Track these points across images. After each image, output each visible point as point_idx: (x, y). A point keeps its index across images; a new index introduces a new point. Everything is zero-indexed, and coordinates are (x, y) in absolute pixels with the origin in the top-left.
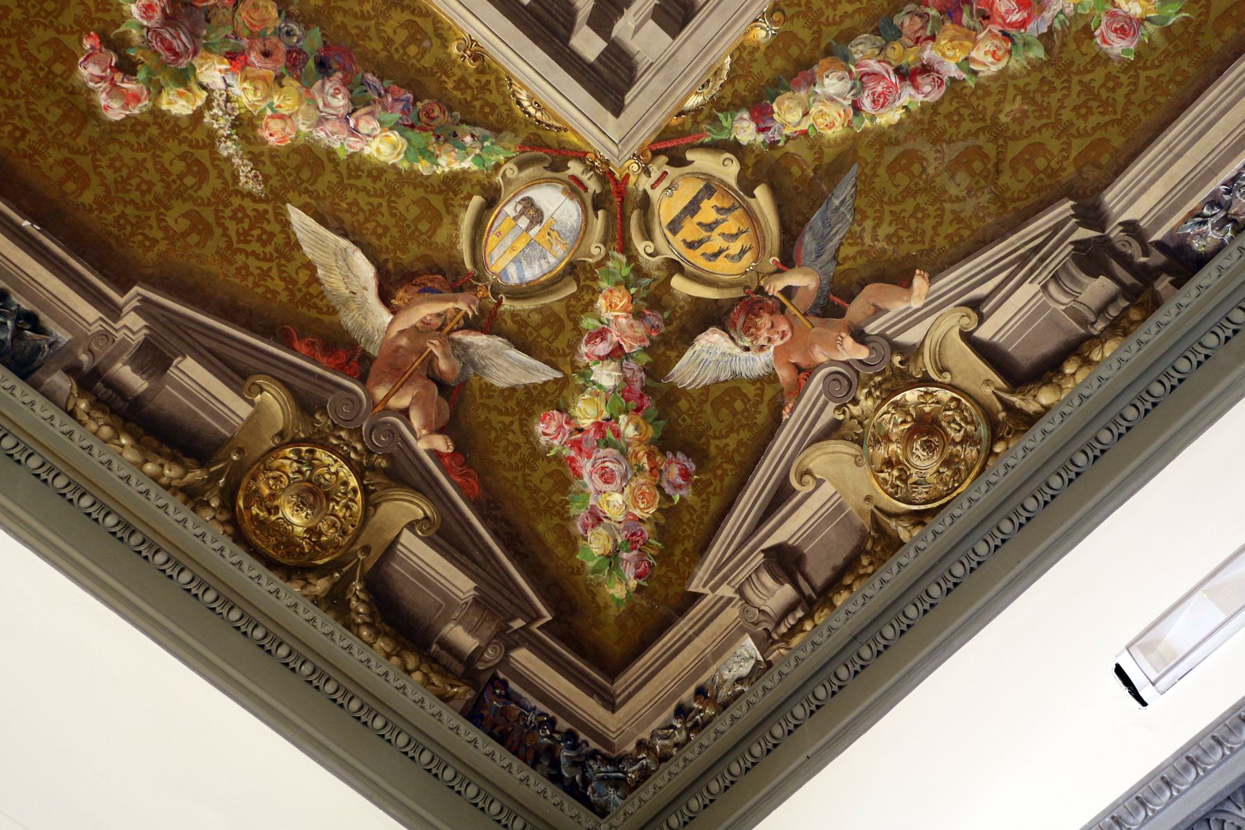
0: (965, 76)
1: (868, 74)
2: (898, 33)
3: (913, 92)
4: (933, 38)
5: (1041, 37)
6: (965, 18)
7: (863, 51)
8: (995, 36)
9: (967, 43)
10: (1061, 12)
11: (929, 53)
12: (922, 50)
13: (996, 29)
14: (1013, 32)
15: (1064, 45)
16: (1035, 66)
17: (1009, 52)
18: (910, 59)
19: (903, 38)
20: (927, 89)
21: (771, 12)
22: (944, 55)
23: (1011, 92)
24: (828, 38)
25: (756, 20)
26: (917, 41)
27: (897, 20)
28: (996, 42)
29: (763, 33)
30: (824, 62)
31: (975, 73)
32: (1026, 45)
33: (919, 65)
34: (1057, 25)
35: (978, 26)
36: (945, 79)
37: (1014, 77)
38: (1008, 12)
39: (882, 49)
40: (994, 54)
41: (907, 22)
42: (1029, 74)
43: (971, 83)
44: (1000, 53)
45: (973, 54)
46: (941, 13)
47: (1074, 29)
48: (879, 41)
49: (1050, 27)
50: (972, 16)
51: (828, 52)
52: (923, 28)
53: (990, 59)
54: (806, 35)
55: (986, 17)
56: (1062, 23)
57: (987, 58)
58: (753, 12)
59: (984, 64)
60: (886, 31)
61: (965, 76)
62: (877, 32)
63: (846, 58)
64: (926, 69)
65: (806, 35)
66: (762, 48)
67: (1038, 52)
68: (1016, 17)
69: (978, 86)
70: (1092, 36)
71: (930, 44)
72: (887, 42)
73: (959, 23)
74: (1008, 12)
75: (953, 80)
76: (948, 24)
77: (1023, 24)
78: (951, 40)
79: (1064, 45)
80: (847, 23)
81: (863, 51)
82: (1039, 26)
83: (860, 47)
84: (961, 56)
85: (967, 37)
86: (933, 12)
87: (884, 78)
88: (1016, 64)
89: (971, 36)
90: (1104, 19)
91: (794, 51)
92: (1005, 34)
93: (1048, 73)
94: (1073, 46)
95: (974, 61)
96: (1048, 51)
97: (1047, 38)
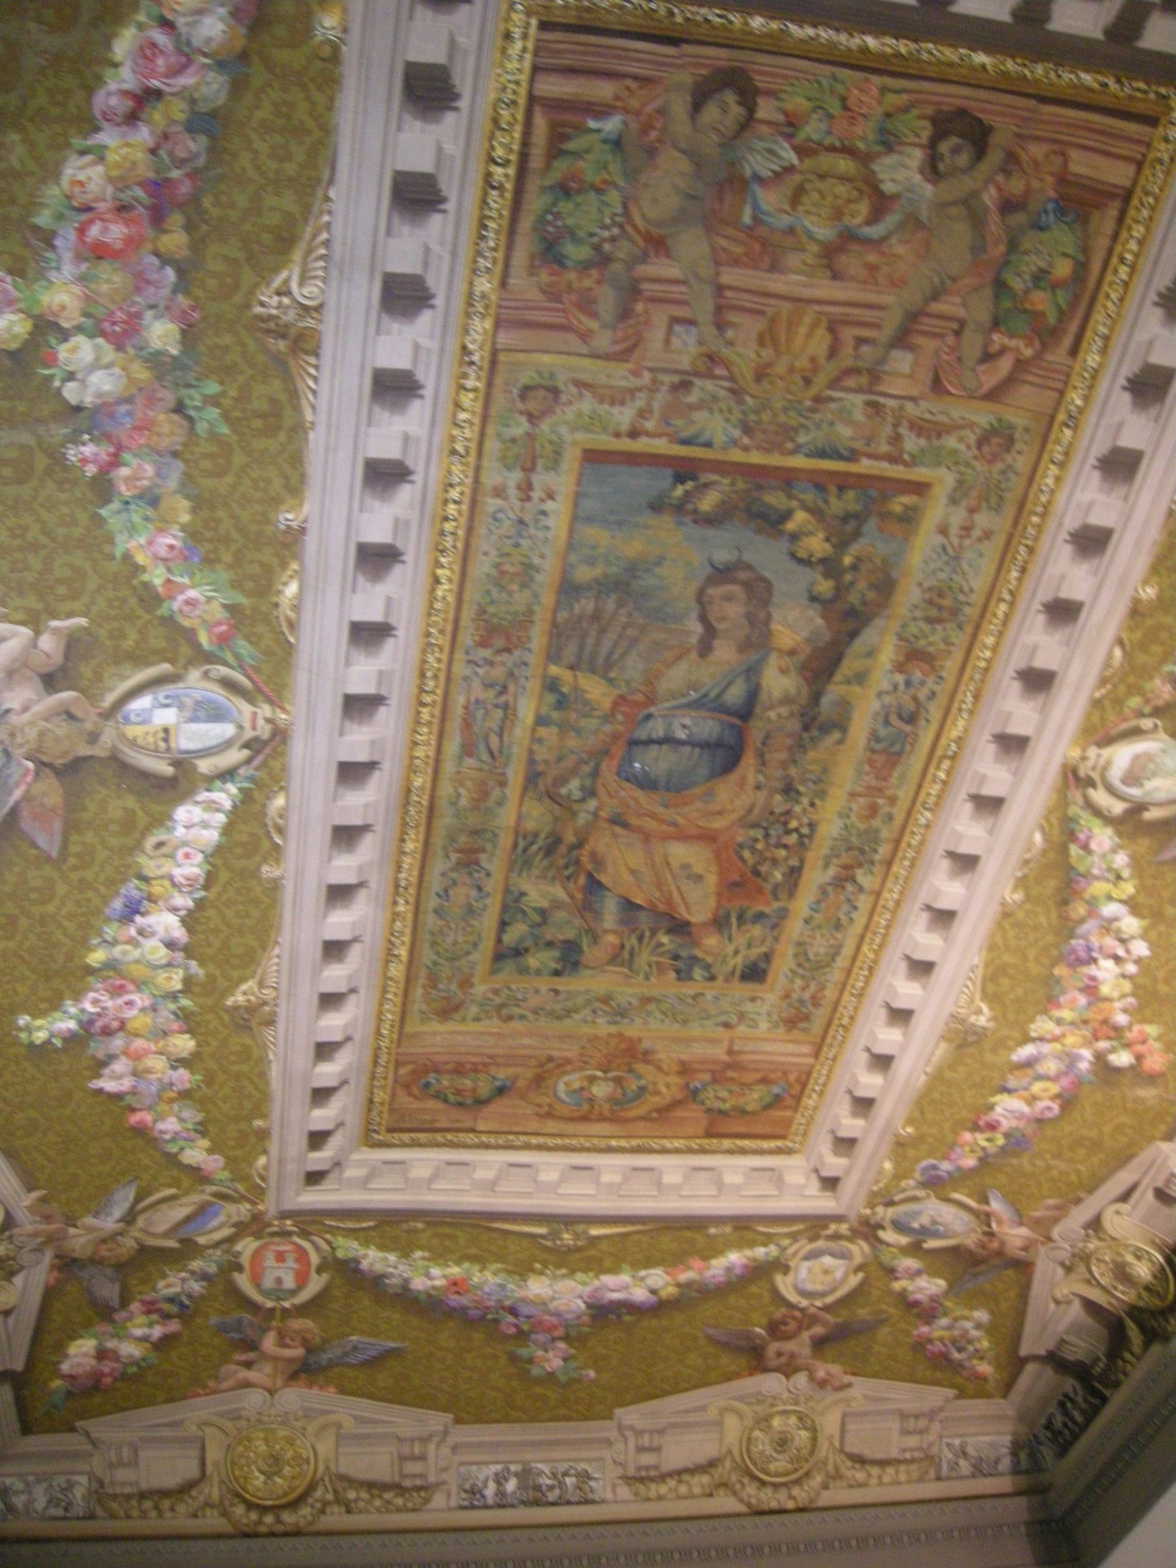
0: (89, 143)
1: (185, 67)
2: (191, 128)
3: (126, 86)
4: (153, 151)
5: (54, 234)
6: (139, 192)
7: (212, 87)
8: (97, 200)
9: (115, 173)
10: (58, 269)
11: (144, 135)
12: (153, 133)
13: (102, 206)
14: (84, 217)
15: (28, 245)
16: (34, 205)
17: (68, 197)
18: (157, 114)
19: (180, 128)
20: (114, 101)
21: (335, 57)
22: (128, 145)
23: (31, 166)
24: (258, 75)
25: (345, 31)
26: (166, 137)
27: (203, 140)
28: (89, 197)
29: (327, 24)
30: (240, 43)
31: (83, 153)
32: (60, 217)
33: (143, 116)
34: (49, 255)
35: (122, 196)
36: (105, 125)
37: (43, 181)
38: (105, 230)
39: (193, 101)
40: (81, 184)
41: (192, 146)
42: (32, 195)
43: (77, 142)
44: (77, 189)
45: (100, 169)
46: (167, 180)
47: (32, 264)
48: (203, 108)
49: (53, 247)
50: (136, 199)
51: (244, 57)
52: (171, 154)
53: (81, 177)
54: (281, 56)
55: (122, 209)
56: (47, 261)
57: (85, 175)
58: (355, 36)
59: (81, 168)
60: (205, 121)
61: (89, 143)
62: (213, 114)
63: (221, 65)
64: (132, 118)
65: (281, 56)
66: (315, 7)
67: (43, 219)
68: (94, 231)
69: (68, 145)
70: (11, 272)
71: (151, 143)
72: (194, 113)
73: (141, 184)
74: (105, 230)
75: (97, 129)
76: (151, 175)
77: (82, 231)
78: (134, 164)
79: (28, 245)
80: (249, 99)
81: (212, 87)
82: (66, 239)
83: (215, 87)
84: (112, 157)
85: (121, 178)
86: (175, 174)
87: (167, 76)
88: (53, 193)
89: (119, 182)
90: (15, 294)
91: (280, 31)
92: (89, 209)
93: (15, 212)
94: (19, 251)
95: (94, 163)
96: (36, 229)
97: (48, 238)
